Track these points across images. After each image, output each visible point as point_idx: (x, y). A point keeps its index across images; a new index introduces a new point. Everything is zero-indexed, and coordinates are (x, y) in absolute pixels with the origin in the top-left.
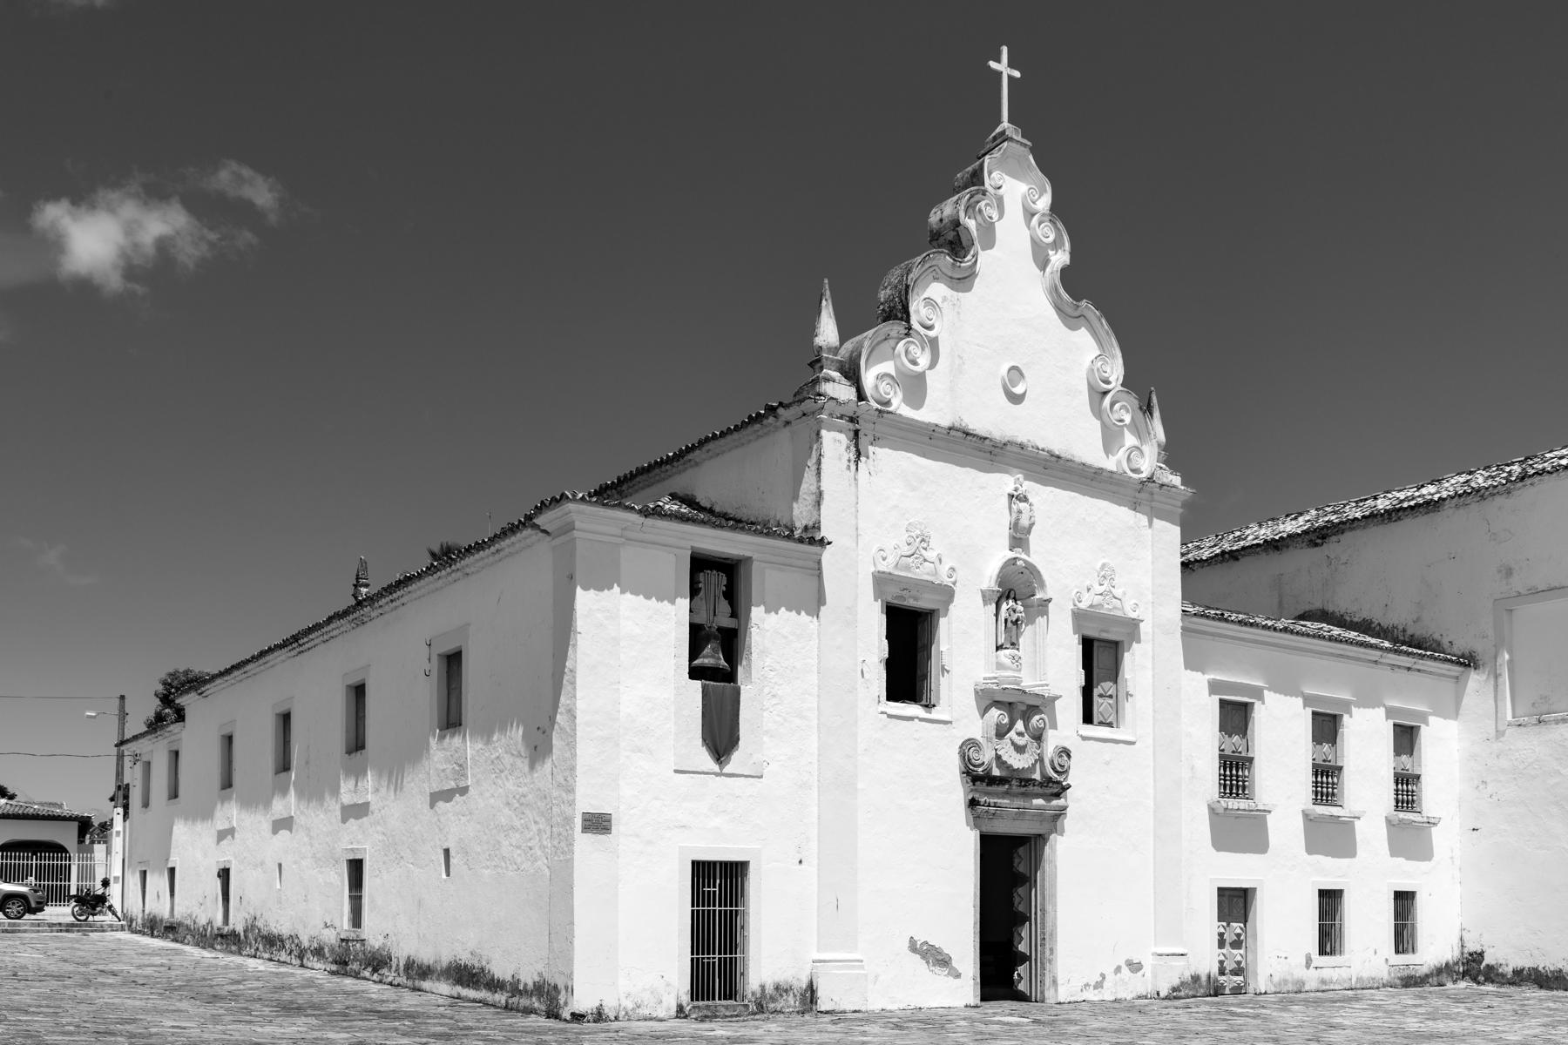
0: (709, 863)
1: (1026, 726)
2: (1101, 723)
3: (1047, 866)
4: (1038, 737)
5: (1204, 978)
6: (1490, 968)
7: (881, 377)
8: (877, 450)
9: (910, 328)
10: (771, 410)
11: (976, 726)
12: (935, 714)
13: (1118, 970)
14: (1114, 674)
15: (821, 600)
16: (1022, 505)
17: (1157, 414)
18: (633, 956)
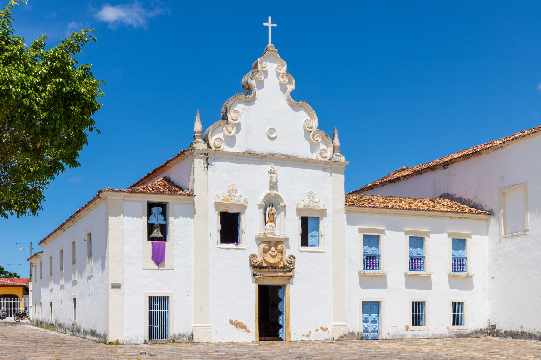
1: (276, 249)
2: (312, 246)
3: (286, 295)
4: (281, 252)
5: (356, 334)
6: (498, 331)
7: (216, 139)
8: (216, 163)
9: (228, 122)
10: (182, 152)
11: (256, 250)
12: (240, 247)
13: (317, 330)
14: (317, 229)
15: (194, 213)
16: (273, 175)
17: (336, 136)
18: (132, 326)
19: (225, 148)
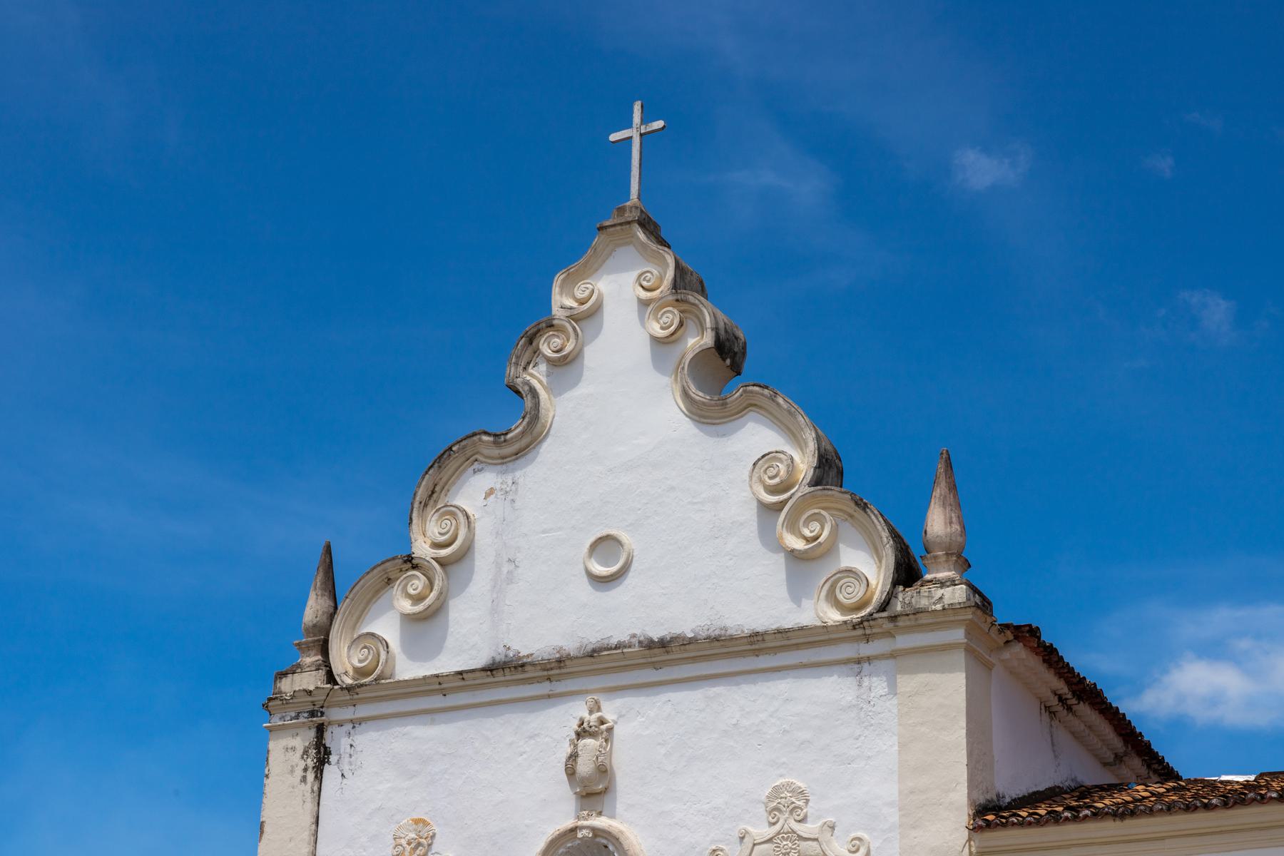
19: (407, 670)
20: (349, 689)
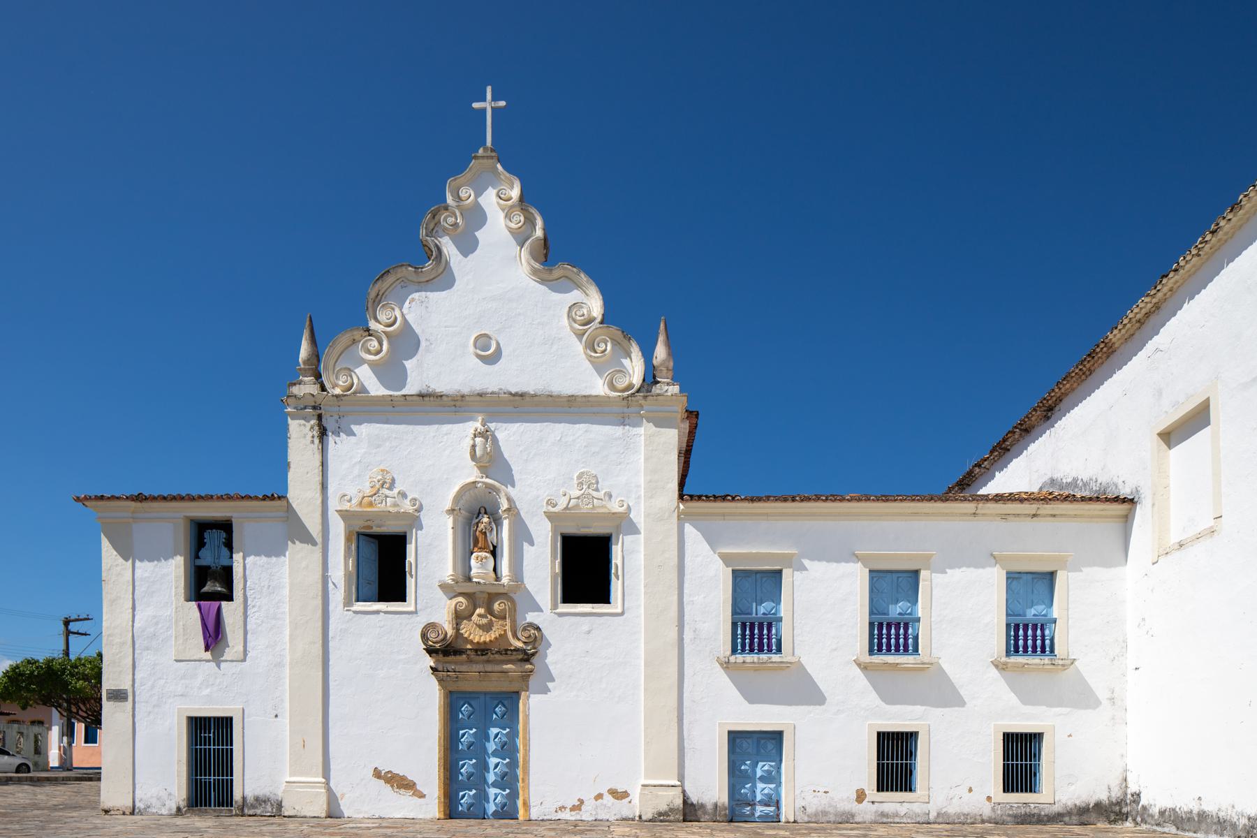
0: (205, 718)
5: (709, 807)
19: (376, 388)
20: (337, 396)
